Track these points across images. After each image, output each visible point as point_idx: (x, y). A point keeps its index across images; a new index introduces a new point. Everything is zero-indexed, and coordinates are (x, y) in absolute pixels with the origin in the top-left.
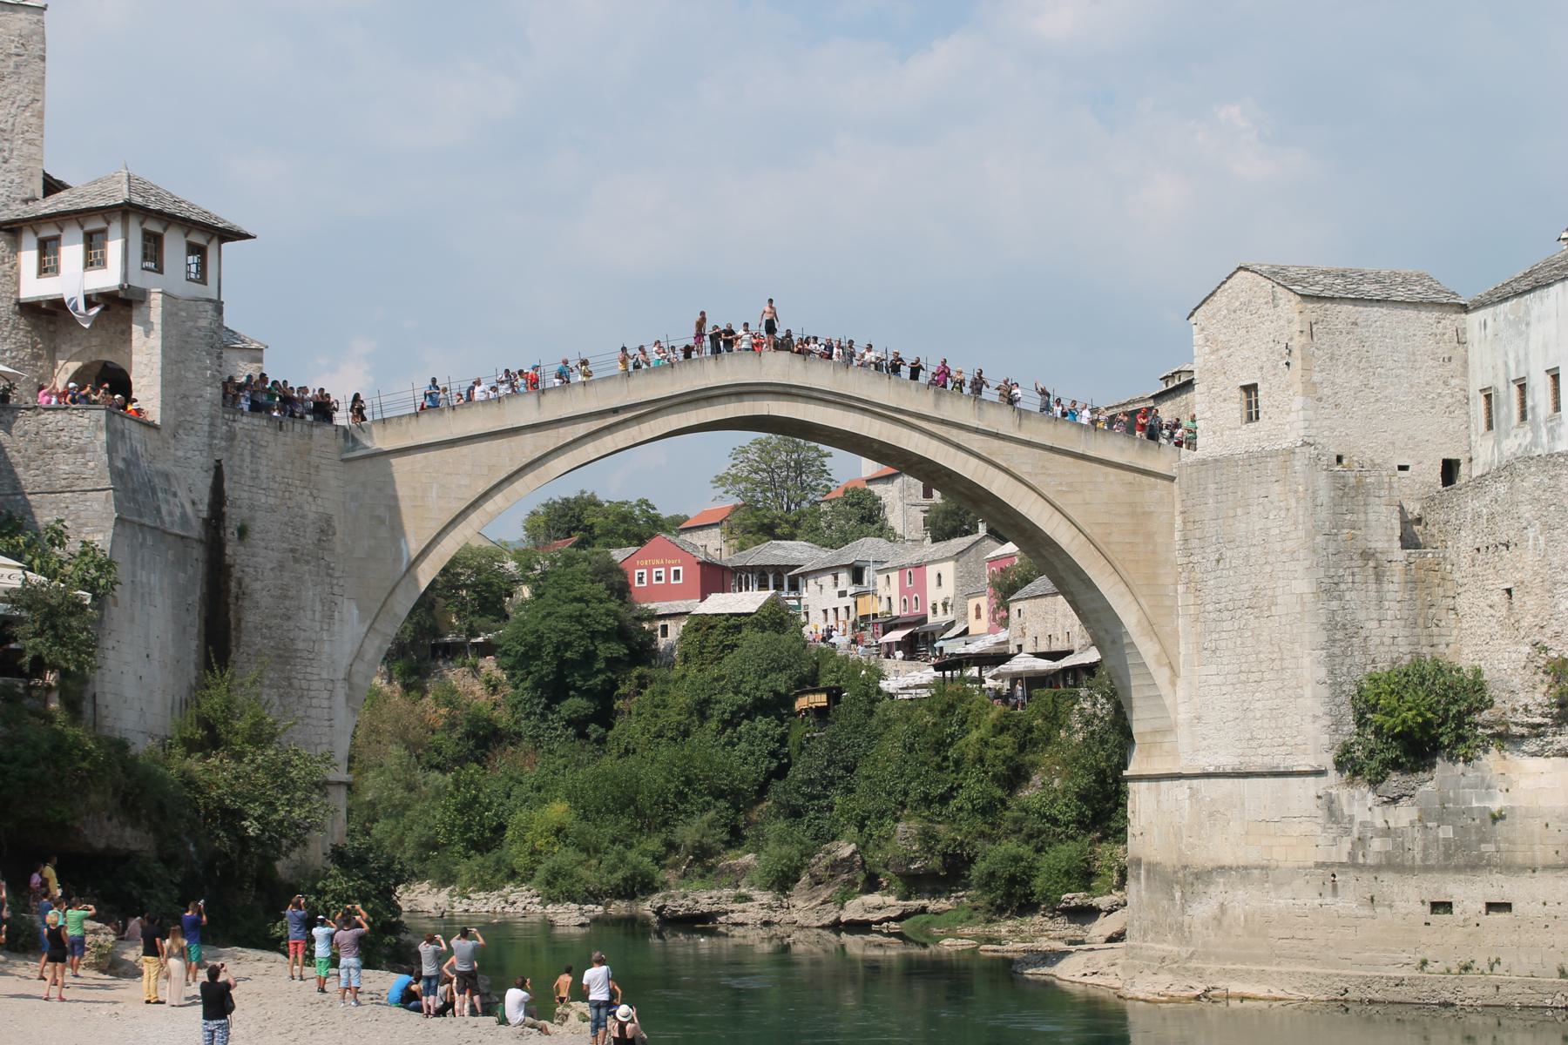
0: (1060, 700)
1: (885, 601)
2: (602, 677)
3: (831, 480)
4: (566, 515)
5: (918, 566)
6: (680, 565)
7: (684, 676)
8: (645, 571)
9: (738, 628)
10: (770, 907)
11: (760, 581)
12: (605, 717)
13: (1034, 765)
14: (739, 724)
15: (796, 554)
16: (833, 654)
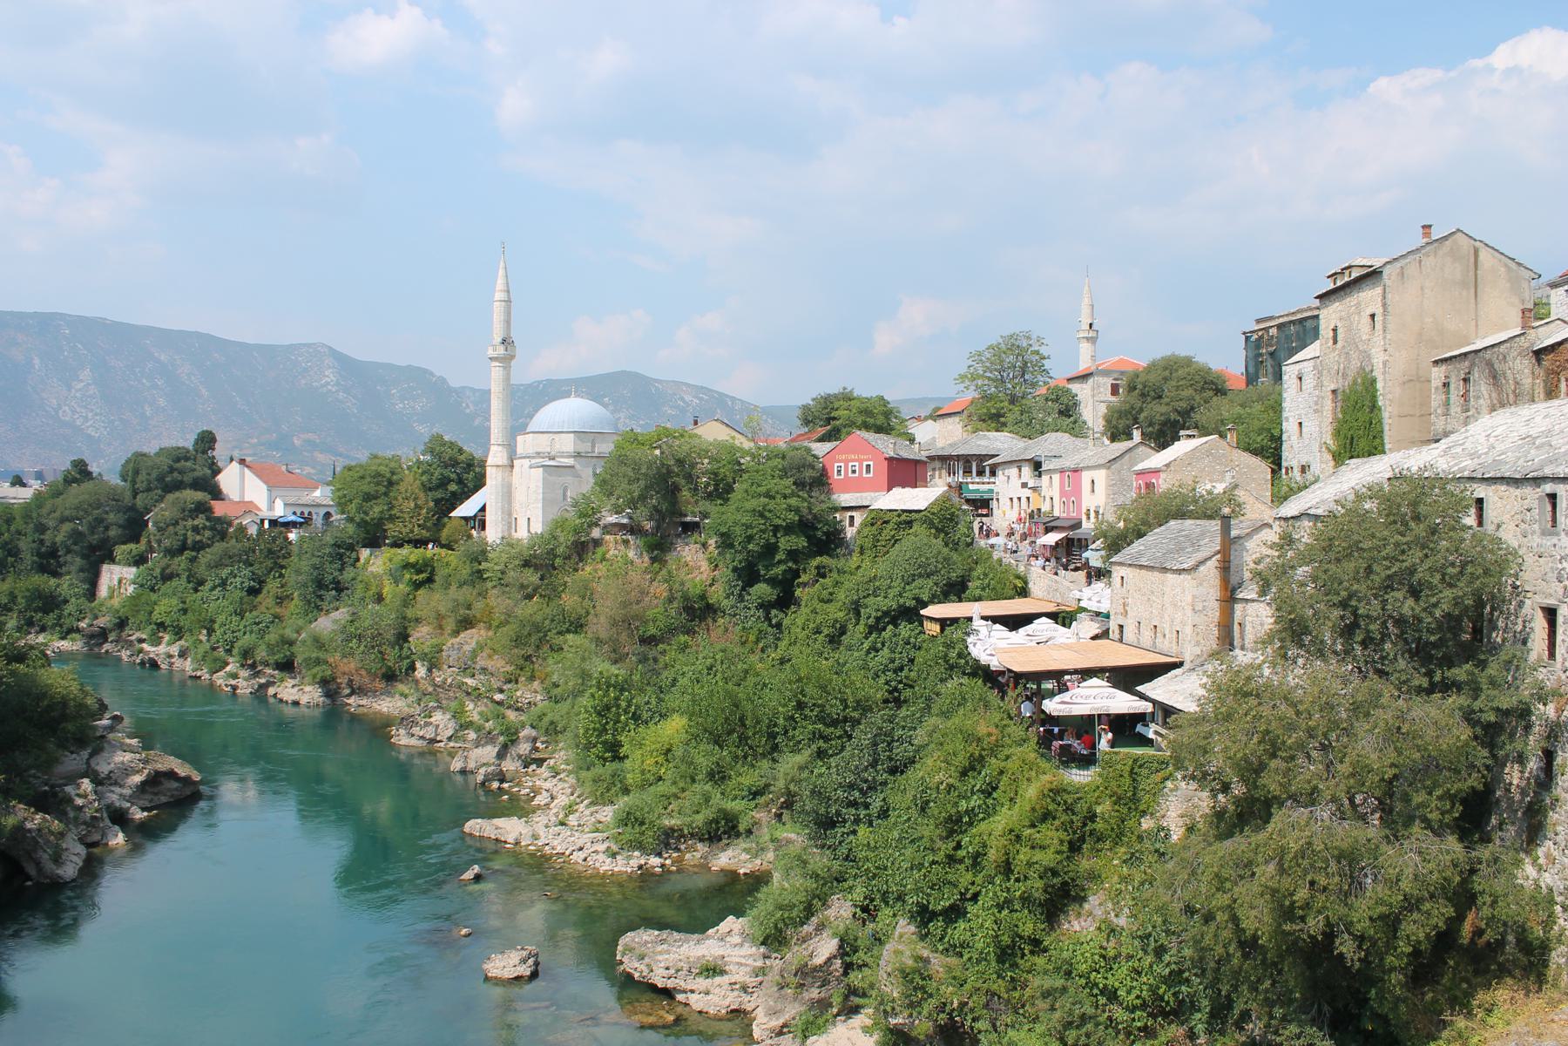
0: (1144, 772)
1: (1048, 500)
2: (783, 567)
3: (1051, 378)
4: (826, 408)
5: (1075, 471)
6: (870, 460)
7: (859, 567)
8: (842, 464)
9: (909, 524)
10: (744, 989)
11: (965, 468)
12: (786, 600)
13: (1094, 876)
14: (884, 629)
15: (999, 445)
16: (990, 556)
